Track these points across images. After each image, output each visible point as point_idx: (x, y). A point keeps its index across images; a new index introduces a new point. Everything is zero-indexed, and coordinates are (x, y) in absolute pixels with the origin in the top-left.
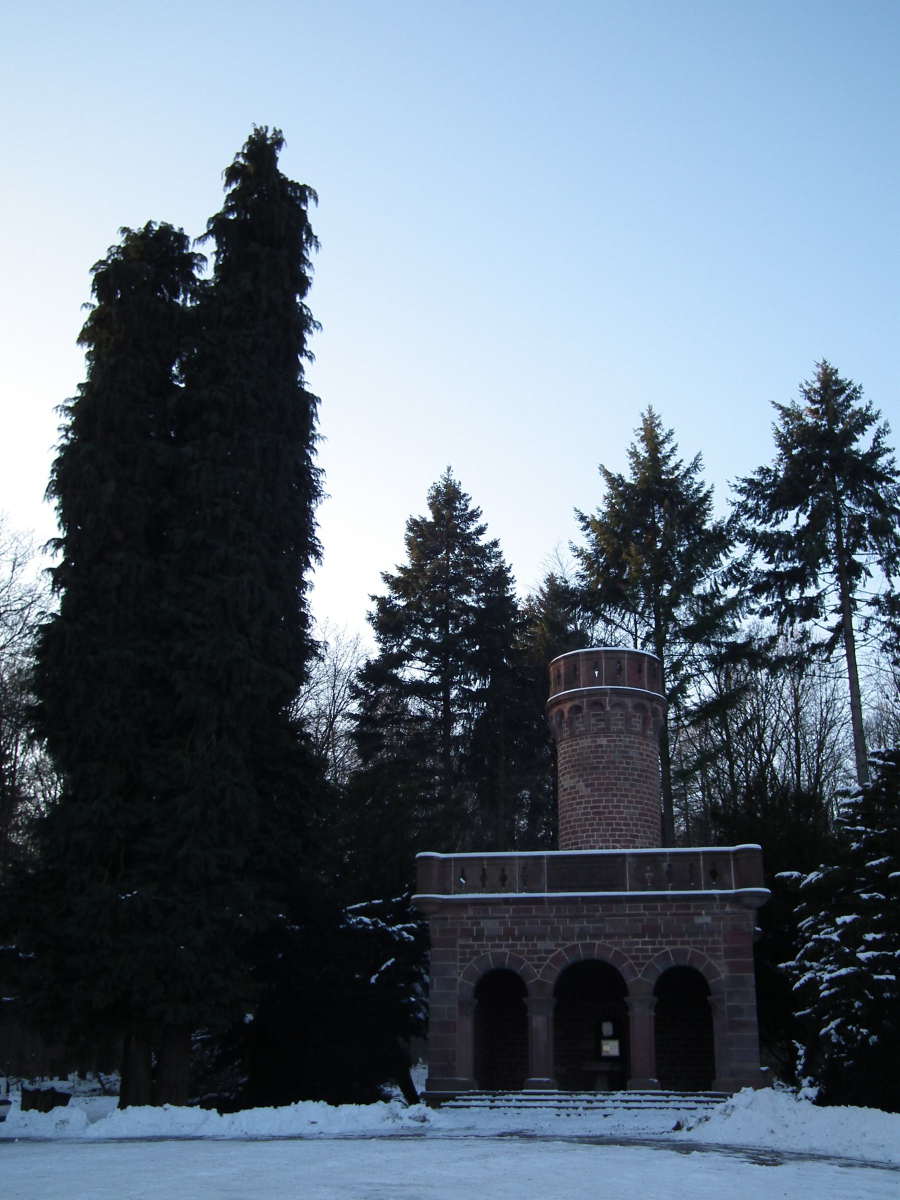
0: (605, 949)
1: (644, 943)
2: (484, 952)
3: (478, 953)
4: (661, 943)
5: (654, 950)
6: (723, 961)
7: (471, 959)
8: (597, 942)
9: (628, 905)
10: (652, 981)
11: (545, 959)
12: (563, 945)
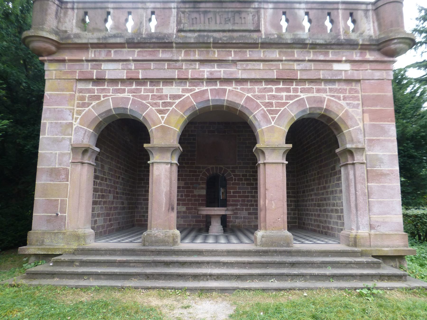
0: (235, 95)
1: (278, 90)
2: (104, 97)
3: (98, 98)
4: (296, 90)
5: (289, 98)
6: (360, 110)
7: (89, 104)
8: (228, 88)
9: (262, 50)
10: (285, 128)
11: (170, 104)
12: (191, 90)
